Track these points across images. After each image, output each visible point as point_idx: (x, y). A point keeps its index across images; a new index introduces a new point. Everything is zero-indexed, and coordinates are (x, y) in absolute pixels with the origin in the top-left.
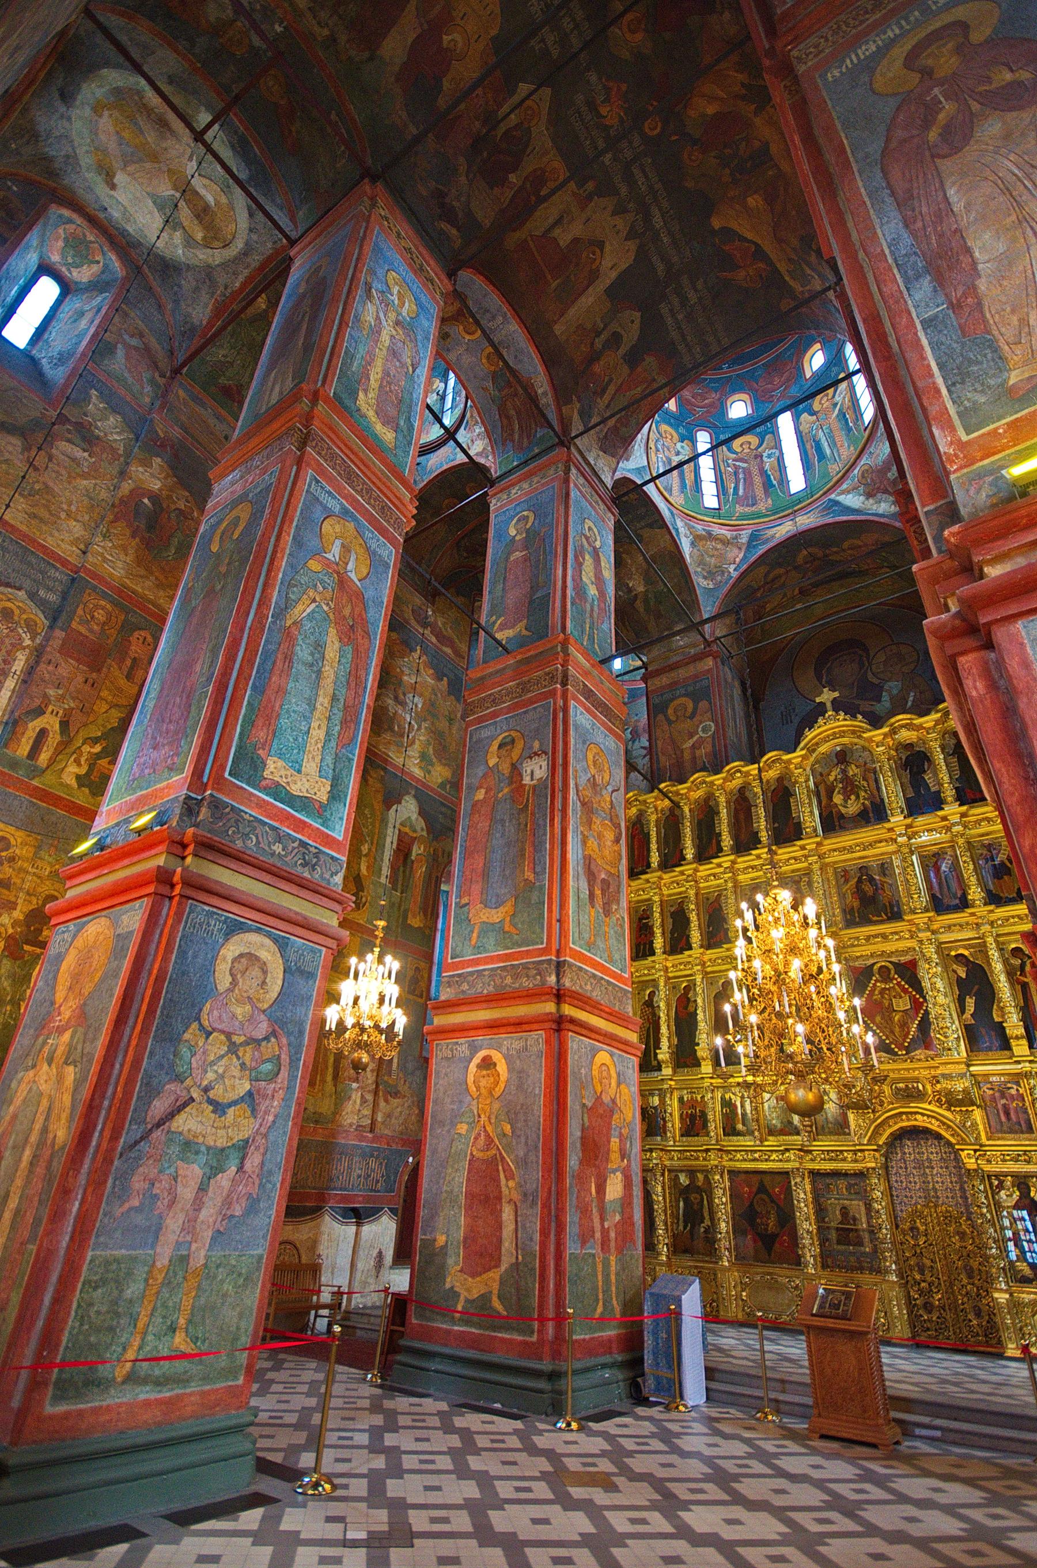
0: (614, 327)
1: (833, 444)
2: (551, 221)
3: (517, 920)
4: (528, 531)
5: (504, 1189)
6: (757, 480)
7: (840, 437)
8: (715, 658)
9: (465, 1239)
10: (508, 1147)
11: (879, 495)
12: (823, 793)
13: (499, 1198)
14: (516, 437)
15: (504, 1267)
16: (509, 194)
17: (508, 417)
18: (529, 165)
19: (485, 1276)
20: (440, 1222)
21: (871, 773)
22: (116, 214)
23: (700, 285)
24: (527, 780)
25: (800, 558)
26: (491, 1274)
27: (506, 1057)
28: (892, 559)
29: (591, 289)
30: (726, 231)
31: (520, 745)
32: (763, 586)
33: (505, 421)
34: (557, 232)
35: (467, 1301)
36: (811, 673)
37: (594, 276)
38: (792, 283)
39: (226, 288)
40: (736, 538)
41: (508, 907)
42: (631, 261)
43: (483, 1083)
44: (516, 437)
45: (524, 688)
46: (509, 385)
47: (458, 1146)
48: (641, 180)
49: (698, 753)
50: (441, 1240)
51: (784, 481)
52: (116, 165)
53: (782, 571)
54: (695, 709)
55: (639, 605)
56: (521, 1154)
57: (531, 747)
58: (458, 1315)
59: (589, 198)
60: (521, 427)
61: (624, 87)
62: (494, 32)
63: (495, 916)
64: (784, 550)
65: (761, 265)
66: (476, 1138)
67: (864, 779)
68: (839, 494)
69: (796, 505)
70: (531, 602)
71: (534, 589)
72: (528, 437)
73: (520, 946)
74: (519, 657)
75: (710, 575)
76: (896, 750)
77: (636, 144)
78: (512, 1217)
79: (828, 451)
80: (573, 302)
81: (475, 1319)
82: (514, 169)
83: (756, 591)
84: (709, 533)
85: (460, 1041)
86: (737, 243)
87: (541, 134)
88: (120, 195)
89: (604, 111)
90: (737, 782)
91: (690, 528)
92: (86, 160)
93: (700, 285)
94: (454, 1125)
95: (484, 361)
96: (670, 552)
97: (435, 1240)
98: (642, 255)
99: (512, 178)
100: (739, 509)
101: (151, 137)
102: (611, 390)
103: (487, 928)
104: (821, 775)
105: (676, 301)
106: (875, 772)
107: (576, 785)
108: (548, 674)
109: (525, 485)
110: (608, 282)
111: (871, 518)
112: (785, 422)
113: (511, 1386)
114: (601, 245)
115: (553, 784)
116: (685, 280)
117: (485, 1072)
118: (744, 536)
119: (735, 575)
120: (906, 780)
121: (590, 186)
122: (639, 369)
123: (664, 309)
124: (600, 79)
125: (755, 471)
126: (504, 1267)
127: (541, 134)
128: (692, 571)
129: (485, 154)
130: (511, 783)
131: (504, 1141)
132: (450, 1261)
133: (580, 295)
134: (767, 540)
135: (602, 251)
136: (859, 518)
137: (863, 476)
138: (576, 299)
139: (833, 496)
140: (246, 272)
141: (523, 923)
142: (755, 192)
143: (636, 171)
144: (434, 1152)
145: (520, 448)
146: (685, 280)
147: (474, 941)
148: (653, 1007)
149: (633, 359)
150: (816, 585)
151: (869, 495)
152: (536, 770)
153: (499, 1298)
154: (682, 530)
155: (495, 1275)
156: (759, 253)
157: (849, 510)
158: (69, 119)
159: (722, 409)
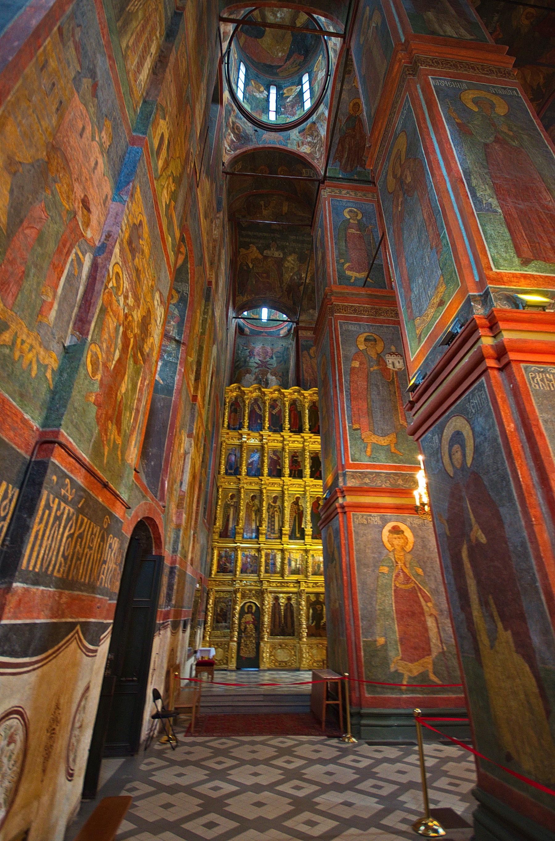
3: (399, 447)
4: (358, 221)
5: (425, 607)
9: (401, 640)
10: (424, 583)
13: (422, 613)
15: (434, 654)
19: (421, 661)
20: (378, 628)
24: (390, 366)
26: (425, 660)
27: (411, 528)
33: (340, 148)
35: (410, 678)
41: (392, 437)
43: (396, 542)
44: (344, 161)
45: (377, 312)
47: (383, 581)
50: (381, 640)
55: (302, 288)
56: (433, 587)
57: (390, 349)
58: (404, 688)
63: (384, 441)
66: (397, 576)
72: (351, 167)
73: (405, 463)
74: (369, 292)
78: (435, 625)
81: (418, 688)
85: (373, 514)
94: (376, 567)
95: (351, 104)
97: (376, 641)
103: (376, 448)
109: (353, 194)
113: (447, 726)
117: (396, 536)
126: (434, 654)
131: (419, 578)
132: (392, 654)
141: (404, 450)
144: (364, 583)
147: (369, 454)
148: (298, 505)
153: (434, 673)
155: (429, 660)
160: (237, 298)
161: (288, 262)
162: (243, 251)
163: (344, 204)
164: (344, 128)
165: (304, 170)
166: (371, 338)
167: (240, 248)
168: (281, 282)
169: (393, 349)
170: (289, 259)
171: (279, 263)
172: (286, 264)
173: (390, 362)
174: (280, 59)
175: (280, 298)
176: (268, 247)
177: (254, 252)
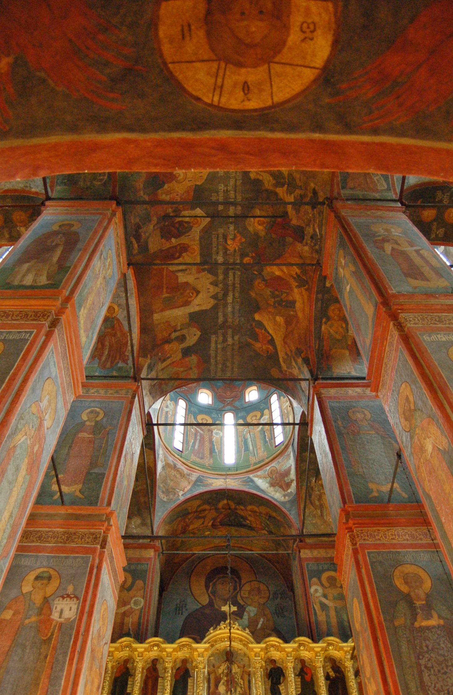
0: (185, 332)
1: (254, 445)
4: (97, 423)
6: (207, 444)
7: (260, 443)
8: (155, 551)
11: (277, 488)
12: (212, 681)
14: (104, 358)
16: (168, 246)
17: (103, 345)
18: (184, 240)
21: (248, 675)
23: (236, 338)
24: (55, 616)
25: (220, 505)
28: (271, 527)
29: (182, 308)
30: (260, 325)
31: (55, 583)
32: (195, 512)
33: (100, 346)
34: (179, 274)
36: (203, 583)
37: (187, 303)
38: (282, 363)
40: (189, 475)
42: (208, 308)
44: (104, 358)
45: (70, 537)
48: (231, 278)
49: (126, 620)
51: (221, 452)
53: (207, 507)
54: (133, 584)
59: (203, 270)
60: (109, 354)
61: (244, 240)
62: (199, 183)
64: (215, 495)
65: (271, 347)
67: (242, 678)
68: (255, 476)
69: (226, 472)
70: (88, 473)
71: (93, 464)
72: (112, 363)
74: (70, 511)
75: (166, 492)
76: (266, 662)
79: (251, 448)
80: (170, 309)
82: (177, 237)
83: (189, 513)
84: (175, 466)
86: (263, 331)
87: (196, 232)
89: (229, 242)
90: (154, 654)
91: (165, 457)
93: (236, 338)
96: (149, 468)
98: (215, 308)
99: (173, 240)
100: (193, 458)
102: (168, 362)
104: (214, 666)
105: (221, 338)
106: (249, 675)
107: (93, 632)
108: (93, 534)
109: (102, 392)
110: (192, 311)
111: (270, 499)
112: (229, 418)
114: (198, 292)
115: (79, 627)
116: (230, 331)
118: (194, 477)
119: (182, 499)
120: (268, 687)
122: (187, 359)
123: (213, 338)
124: (235, 230)
125: (207, 438)
127: (196, 232)
128: (157, 485)
129: (167, 223)
130: (40, 613)
133: (176, 308)
134: (207, 485)
135: (197, 295)
136: (263, 496)
137: (271, 473)
138: (173, 308)
139: (251, 476)
142: (282, 316)
143: (231, 274)
145: (103, 366)
146: (230, 331)
149: (186, 352)
150: (223, 524)
151: (272, 485)
152: (65, 610)
154: (161, 456)
156: (272, 341)
157: (257, 488)
159: (195, 393)
163: (87, 404)
166: (46, 575)
169: (70, 589)
173: (59, 609)
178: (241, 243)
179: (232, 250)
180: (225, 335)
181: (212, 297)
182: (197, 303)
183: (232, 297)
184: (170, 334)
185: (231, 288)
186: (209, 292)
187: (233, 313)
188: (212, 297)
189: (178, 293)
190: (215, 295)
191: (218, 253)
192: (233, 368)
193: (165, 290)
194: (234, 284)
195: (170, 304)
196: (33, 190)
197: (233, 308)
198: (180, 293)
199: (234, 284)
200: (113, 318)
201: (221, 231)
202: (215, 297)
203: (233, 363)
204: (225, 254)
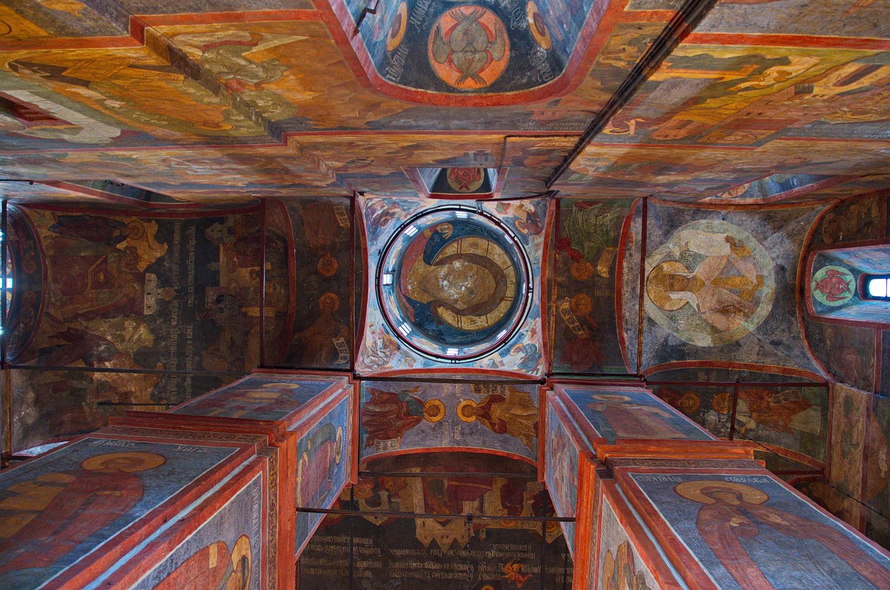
0: (385, 507)
2: (486, 505)
22: (717, 222)
23: (368, 574)
29: (422, 504)
33: (385, 397)
34: (476, 504)
39: (631, 255)
44: (371, 408)
46: (408, 414)
48: (462, 567)
52: (734, 255)
59: (477, 532)
60: (375, 414)
61: (519, 586)
77: (485, 575)
82: (533, 505)
88: (720, 237)
89: (515, 566)
92: (752, 243)
93: (368, 574)
95: (437, 403)
98: (418, 545)
101: (726, 295)
105: (367, 552)
114: (443, 524)
116: (378, 565)
121: (483, 536)
123: (367, 541)
124: (533, 574)
133: (425, 495)
135: (440, 523)
140: (625, 278)
146: (378, 565)
158: (773, 259)
160: (48, 213)
161: (136, 328)
162: (152, 228)
164: (408, 399)
165: (342, 340)
167: (158, 222)
168: (88, 317)
170: (142, 330)
171: (131, 309)
172: (129, 324)
174: (406, 288)
175: (48, 315)
176: (164, 281)
177: (151, 252)
178: (514, 583)
179: (504, 570)
180: (373, 557)
181: (434, 541)
182: (427, 523)
183: (433, 567)
184: (387, 490)
185: (447, 566)
186: (442, 537)
187: (409, 570)
188: (434, 541)
189: (446, 500)
190: (437, 544)
191: (500, 551)
192: (314, 567)
193: (454, 483)
194: (453, 571)
195: (431, 489)
196: (625, 335)
197: (416, 570)
198: (446, 503)
199: (453, 571)
200: (422, 413)
201: (532, 556)
202: (434, 544)
203: (324, 568)
204: (500, 560)
